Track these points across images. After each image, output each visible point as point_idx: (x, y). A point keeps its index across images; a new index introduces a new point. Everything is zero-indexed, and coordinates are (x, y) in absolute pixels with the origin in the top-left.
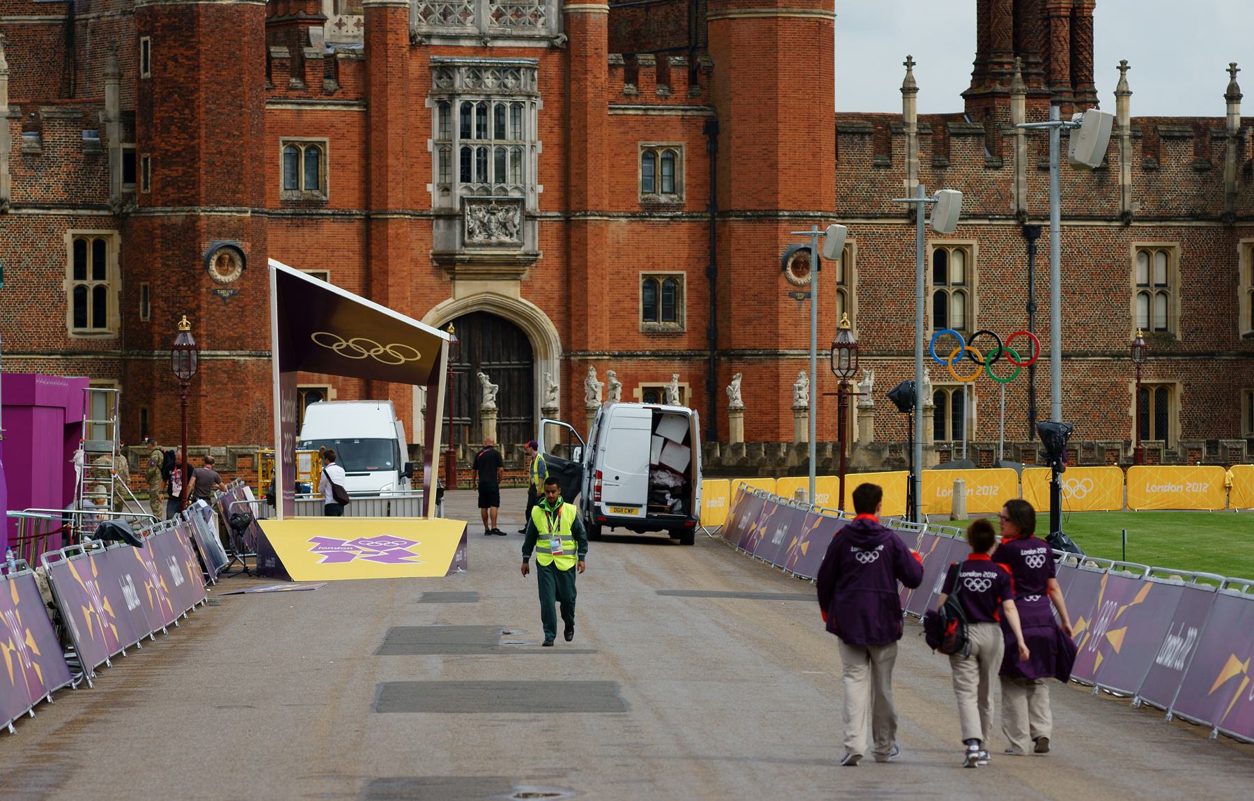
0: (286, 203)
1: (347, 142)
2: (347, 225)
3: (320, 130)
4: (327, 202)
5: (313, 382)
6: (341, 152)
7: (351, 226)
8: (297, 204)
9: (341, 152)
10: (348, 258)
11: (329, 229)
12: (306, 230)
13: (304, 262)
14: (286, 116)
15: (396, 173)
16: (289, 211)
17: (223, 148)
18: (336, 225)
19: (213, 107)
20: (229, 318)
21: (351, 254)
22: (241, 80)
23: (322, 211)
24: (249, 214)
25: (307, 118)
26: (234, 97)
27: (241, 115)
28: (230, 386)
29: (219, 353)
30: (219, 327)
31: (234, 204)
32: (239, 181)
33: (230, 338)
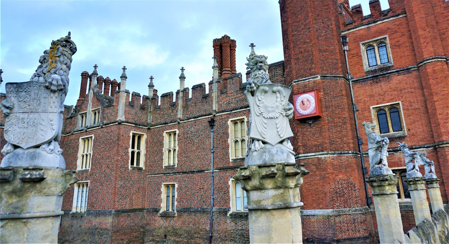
0: (368, 72)
1: (398, 34)
2: (407, 75)
3: (382, 32)
4: (392, 66)
5: (401, 166)
6: (396, 40)
7: (410, 75)
8: (375, 71)
9: (396, 40)
10: (412, 92)
11: (396, 79)
12: (382, 83)
13: (384, 100)
14: (361, 32)
15: (426, 38)
16: (371, 76)
17: (303, 50)
18: (400, 77)
19: (295, 33)
20: (314, 134)
21: (413, 90)
22: (308, 17)
23: (390, 72)
24: (319, 78)
25: (374, 30)
26: (305, 25)
27: (310, 32)
28: (318, 173)
29: (309, 154)
30: (309, 140)
31: (311, 75)
32: (312, 63)
33: (315, 146)
